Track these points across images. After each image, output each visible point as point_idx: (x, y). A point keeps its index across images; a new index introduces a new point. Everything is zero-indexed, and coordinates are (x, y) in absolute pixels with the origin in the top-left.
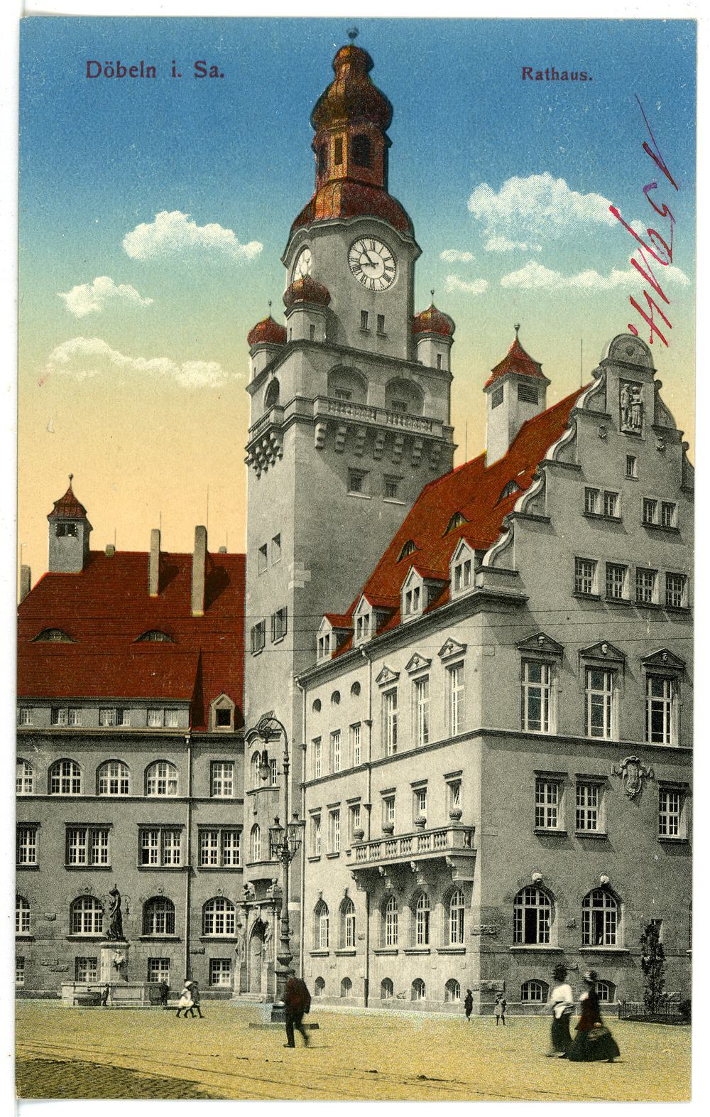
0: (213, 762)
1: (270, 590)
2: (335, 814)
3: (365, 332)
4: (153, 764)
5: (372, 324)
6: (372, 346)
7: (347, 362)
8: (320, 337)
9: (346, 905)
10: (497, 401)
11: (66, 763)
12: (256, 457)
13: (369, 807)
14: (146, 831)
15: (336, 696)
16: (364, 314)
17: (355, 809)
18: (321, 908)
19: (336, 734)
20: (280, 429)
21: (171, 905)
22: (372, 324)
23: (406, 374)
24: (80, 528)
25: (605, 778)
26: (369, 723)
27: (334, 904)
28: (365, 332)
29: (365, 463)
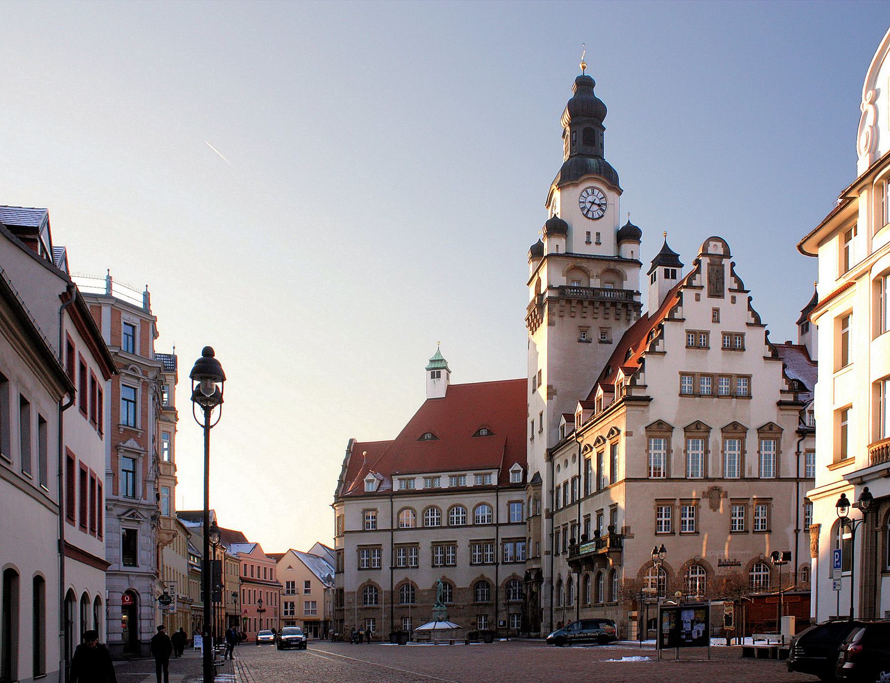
0: (510, 502)
1: (539, 400)
2: (565, 530)
3: (588, 242)
4: (478, 505)
5: (593, 238)
6: (593, 250)
8: (562, 251)
9: (570, 580)
10: (653, 279)
11: (433, 508)
12: (529, 325)
13: (579, 524)
14: (473, 543)
15: (566, 461)
16: (588, 233)
17: (573, 527)
18: (560, 582)
19: (566, 484)
20: (540, 306)
21: (488, 586)
22: (593, 238)
23: (612, 265)
24: (443, 373)
26: (579, 477)
27: (565, 582)
28: (588, 242)
29: (589, 321)
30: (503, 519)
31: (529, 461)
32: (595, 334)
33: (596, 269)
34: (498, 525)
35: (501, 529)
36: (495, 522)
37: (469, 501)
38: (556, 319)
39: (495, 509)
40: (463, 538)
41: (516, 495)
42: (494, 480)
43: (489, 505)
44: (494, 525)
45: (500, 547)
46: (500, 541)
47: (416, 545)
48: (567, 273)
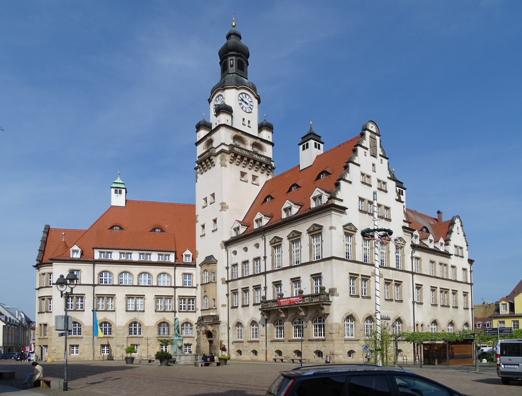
4: (161, 274)
7: (239, 134)
25: (370, 277)
30: (179, 283)
31: (197, 248)
32: (249, 177)
33: (250, 141)
34: (175, 287)
35: (177, 290)
36: (173, 285)
37: (154, 271)
38: (227, 163)
39: (173, 277)
40: (150, 294)
41: (188, 270)
42: (172, 258)
43: (168, 275)
44: (171, 287)
45: (177, 301)
46: (177, 297)
47: (112, 297)
48: (235, 138)
